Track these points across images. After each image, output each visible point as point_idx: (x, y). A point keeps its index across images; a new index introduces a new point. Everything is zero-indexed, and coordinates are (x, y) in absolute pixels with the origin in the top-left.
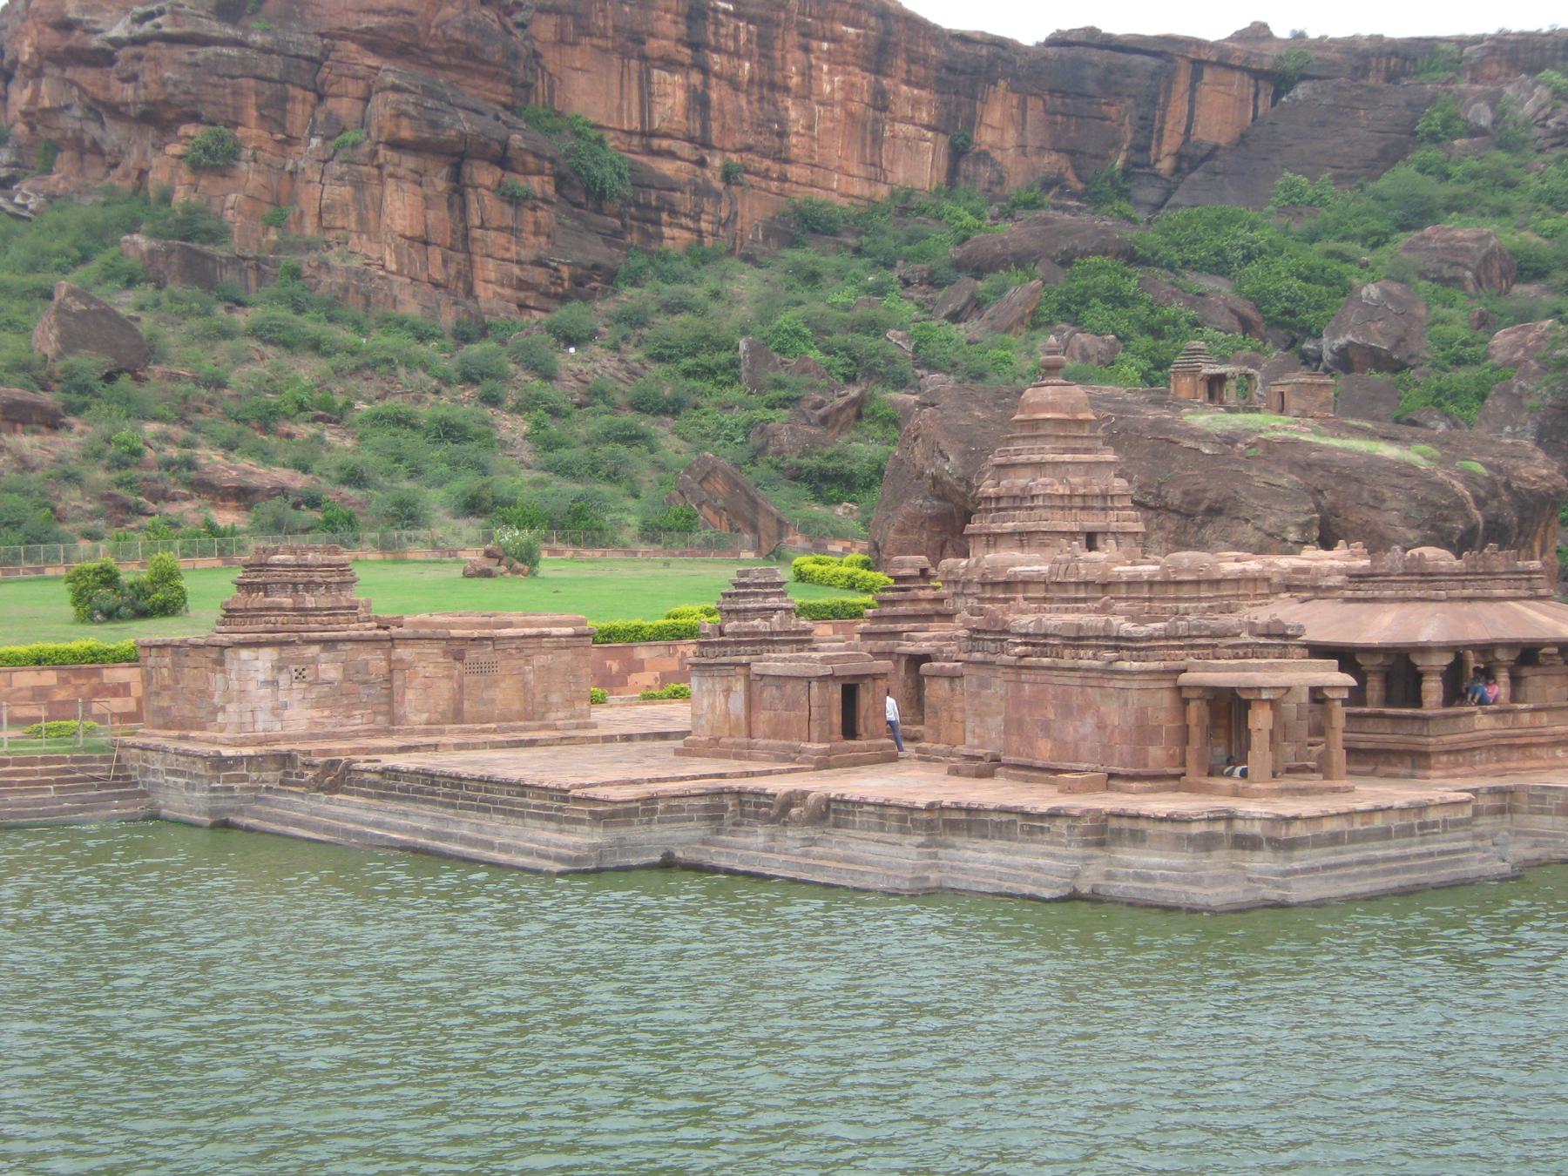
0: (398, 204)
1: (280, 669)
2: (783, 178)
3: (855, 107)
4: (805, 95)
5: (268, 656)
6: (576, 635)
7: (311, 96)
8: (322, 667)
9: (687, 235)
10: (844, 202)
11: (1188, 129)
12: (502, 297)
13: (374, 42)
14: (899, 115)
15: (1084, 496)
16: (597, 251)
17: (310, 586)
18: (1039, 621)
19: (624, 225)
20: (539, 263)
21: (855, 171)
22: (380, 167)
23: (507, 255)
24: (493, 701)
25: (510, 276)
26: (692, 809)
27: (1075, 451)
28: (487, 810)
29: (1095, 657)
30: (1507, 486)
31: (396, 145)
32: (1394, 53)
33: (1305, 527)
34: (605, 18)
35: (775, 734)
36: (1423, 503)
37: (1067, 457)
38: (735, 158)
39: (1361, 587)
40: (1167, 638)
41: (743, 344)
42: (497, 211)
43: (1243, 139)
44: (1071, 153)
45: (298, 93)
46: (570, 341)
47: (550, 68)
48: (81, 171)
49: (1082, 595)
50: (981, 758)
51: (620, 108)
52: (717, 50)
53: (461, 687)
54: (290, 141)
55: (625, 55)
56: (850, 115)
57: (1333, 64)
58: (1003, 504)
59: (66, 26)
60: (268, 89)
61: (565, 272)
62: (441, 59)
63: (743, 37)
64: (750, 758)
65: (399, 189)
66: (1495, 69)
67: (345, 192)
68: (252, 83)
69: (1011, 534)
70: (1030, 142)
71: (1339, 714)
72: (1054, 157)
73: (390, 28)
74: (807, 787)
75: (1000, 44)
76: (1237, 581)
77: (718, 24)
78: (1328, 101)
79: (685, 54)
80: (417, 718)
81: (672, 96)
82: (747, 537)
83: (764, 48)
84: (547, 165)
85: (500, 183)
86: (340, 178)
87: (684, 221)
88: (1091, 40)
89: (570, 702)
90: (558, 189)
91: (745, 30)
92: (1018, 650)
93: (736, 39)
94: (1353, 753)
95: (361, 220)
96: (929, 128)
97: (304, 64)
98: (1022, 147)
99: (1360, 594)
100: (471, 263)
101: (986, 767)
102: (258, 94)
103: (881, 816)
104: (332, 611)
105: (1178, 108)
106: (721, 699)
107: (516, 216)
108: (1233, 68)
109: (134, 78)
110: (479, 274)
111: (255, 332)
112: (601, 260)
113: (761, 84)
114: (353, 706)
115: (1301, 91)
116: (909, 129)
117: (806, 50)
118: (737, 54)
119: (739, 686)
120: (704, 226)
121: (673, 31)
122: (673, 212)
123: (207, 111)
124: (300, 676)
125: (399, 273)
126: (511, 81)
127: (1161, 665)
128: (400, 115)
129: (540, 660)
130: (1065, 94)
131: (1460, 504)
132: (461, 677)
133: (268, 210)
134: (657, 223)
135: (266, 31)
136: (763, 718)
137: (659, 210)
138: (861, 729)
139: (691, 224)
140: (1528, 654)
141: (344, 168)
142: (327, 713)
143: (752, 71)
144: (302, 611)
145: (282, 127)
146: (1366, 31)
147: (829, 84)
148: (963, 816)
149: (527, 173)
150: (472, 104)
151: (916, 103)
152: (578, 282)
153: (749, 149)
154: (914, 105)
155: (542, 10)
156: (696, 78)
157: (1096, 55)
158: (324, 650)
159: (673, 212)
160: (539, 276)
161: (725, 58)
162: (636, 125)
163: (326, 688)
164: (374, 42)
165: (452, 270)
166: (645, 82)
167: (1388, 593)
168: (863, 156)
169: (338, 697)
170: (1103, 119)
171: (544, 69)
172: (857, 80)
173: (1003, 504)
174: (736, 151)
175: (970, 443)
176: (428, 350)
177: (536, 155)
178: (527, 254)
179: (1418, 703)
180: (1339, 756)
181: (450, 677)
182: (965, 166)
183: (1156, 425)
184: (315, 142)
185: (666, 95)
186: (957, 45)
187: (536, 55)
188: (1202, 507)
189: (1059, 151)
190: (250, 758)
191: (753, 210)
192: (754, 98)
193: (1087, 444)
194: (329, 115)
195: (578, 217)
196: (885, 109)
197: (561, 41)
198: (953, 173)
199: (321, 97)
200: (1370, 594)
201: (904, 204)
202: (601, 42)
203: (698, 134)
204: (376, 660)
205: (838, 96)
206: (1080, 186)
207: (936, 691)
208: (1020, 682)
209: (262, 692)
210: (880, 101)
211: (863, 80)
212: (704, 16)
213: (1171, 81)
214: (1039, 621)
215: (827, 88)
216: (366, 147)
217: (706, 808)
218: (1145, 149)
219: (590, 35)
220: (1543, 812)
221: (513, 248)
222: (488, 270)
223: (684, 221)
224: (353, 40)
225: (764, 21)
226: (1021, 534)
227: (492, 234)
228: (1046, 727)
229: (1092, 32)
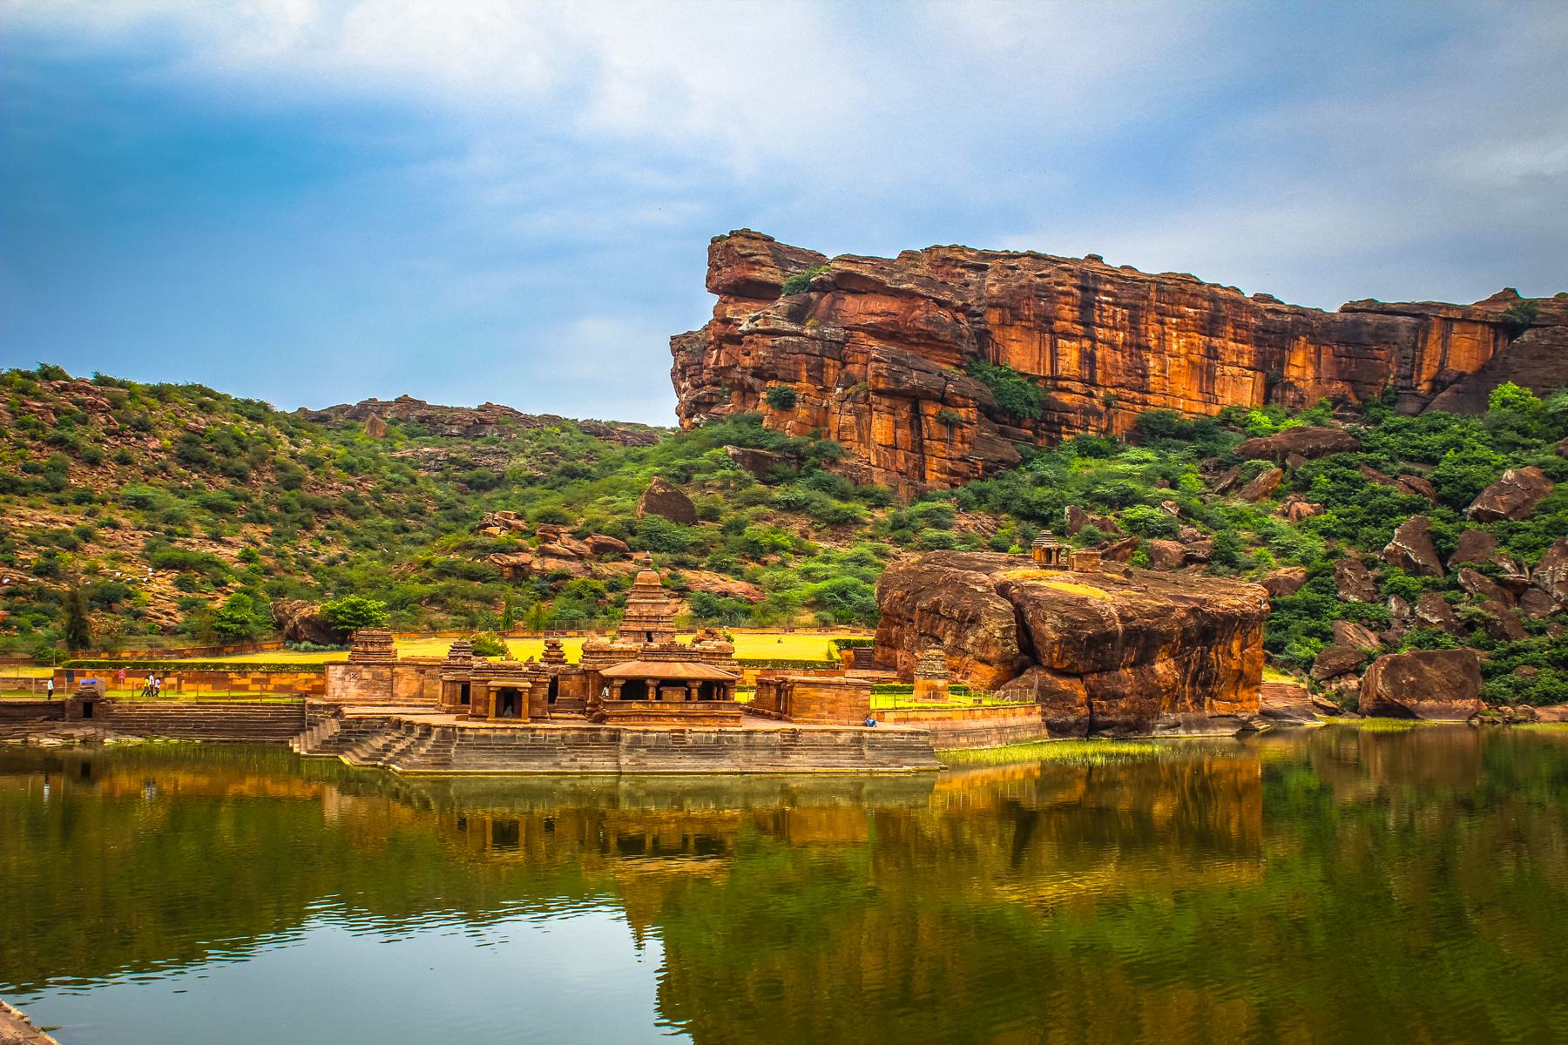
2: (1145, 403)
3: (1194, 358)
4: (1159, 352)
5: (341, 669)
11: (1442, 363)
13: (875, 332)
16: (1007, 450)
17: (372, 644)
19: (1036, 434)
20: (963, 459)
31: (878, 392)
38: (1112, 391)
44: (1351, 381)
45: (831, 362)
48: (743, 402)
54: (826, 390)
55: (1042, 331)
56: (1191, 362)
57: (1553, 316)
59: (727, 322)
63: (1119, 317)
65: (879, 417)
67: (851, 419)
75: (1299, 312)
81: (1070, 354)
88: (1371, 307)
93: (1114, 319)
95: (860, 436)
98: (1317, 379)
104: (380, 653)
105: (1433, 349)
108: (1475, 322)
109: (748, 354)
110: (928, 466)
115: (1527, 336)
116: (1235, 370)
117: (1162, 323)
118: (1115, 328)
121: (1070, 316)
122: (1069, 426)
123: (780, 374)
128: (878, 375)
130: (1348, 344)
133: (811, 430)
134: (1060, 432)
135: (812, 327)
137: (1060, 424)
144: (367, 653)
147: (1177, 344)
151: (1240, 354)
153: (1122, 386)
155: (992, 306)
156: (1086, 344)
157: (1370, 318)
159: (1069, 426)
160: (962, 467)
161: (1107, 331)
162: (1048, 373)
164: (875, 332)
166: (1054, 347)
172: (1196, 341)
178: (955, 454)
184: (839, 390)
189: (1343, 381)
194: (847, 374)
197: (1003, 324)
198: (1267, 398)
199: (845, 364)
204: (386, 672)
205: (1183, 351)
206: (1355, 402)
210: (1212, 354)
211: (1199, 340)
212: (1093, 306)
213: (1426, 333)
215: (1175, 347)
222: (934, 464)
225: (1134, 307)
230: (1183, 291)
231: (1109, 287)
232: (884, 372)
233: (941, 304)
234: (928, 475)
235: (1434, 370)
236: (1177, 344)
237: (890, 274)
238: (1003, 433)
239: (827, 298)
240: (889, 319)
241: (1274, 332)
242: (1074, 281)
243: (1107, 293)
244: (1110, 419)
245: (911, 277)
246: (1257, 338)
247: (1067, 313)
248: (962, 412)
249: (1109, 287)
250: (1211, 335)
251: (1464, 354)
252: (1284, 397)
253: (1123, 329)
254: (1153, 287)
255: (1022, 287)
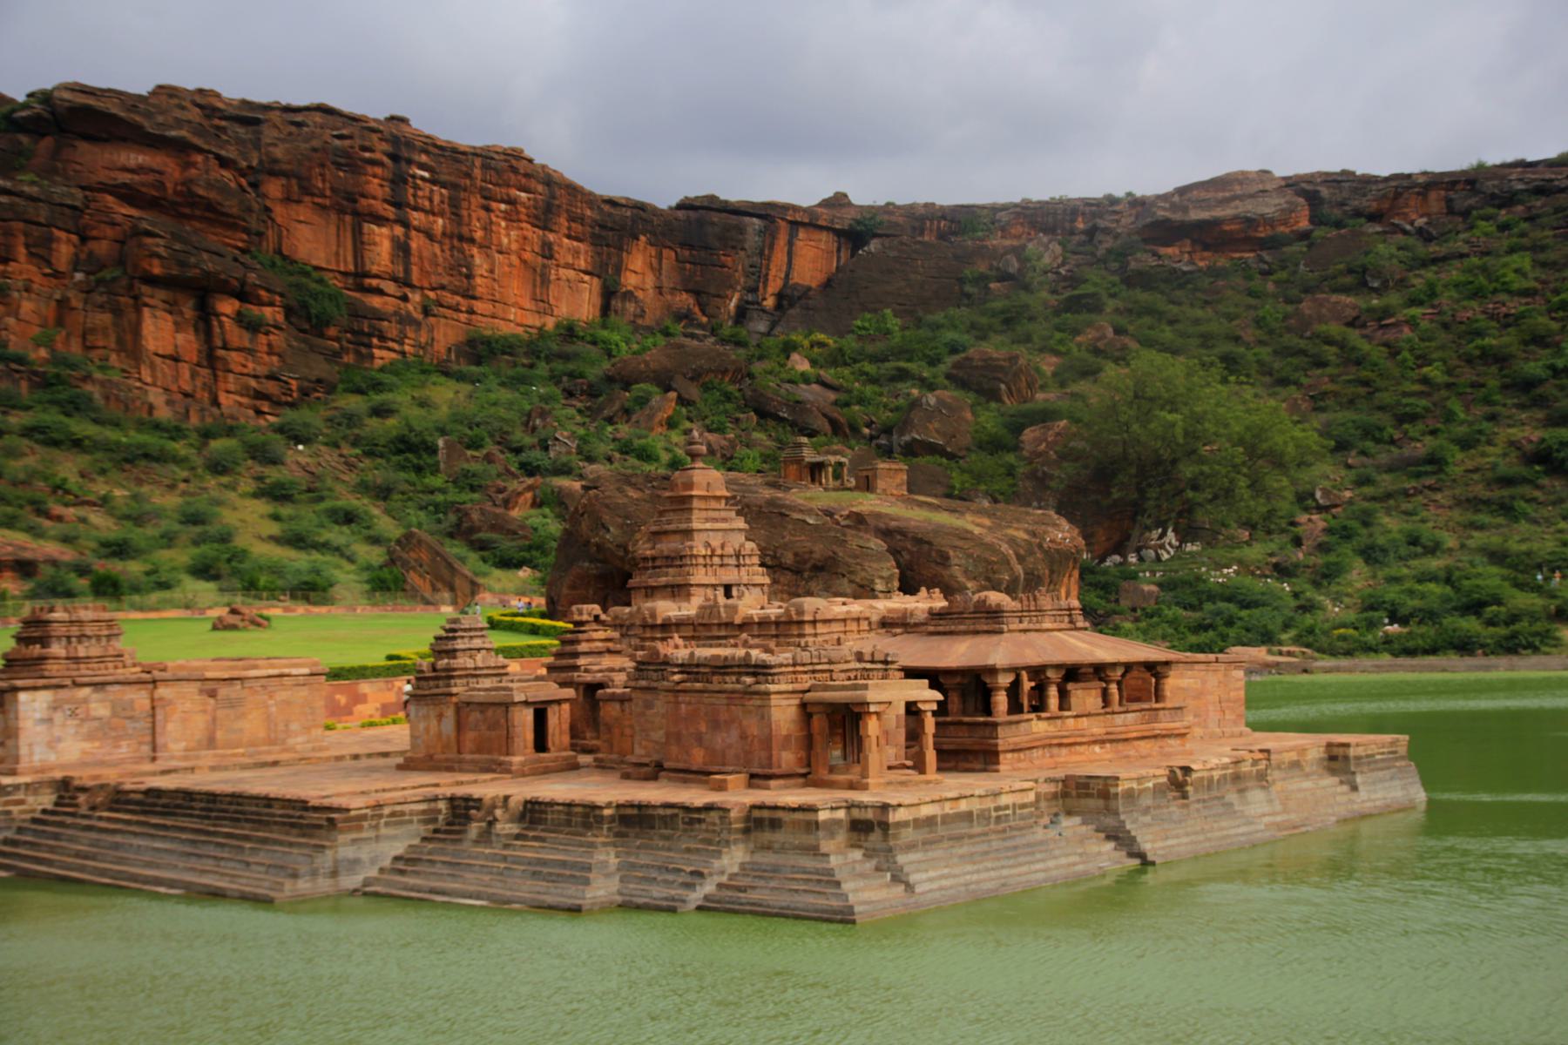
0: (152, 328)
1: (55, 709)
2: (471, 312)
3: (527, 256)
4: (484, 247)
5: (44, 697)
6: (312, 675)
7: (74, 238)
8: (93, 705)
9: (394, 355)
10: (520, 330)
11: (787, 275)
12: (240, 404)
14: (562, 262)
15: (722, 556)
18: (692, 654)
20: (272, 377)
21: (528, 306)
22: (136, 298)
23: (245, 371)
24: (241, 730)
25: (247, 388)
26: (412, 813)
27: (715, 520)
28: (238, 820)
29: (738, 682)
30: (1040, 546)
32: (944, 217)
33: (888, 580)
34: (324, 181)
35: (479, 750)
36: (978, 560)
37: (708, 526)
38: (432, 294)
39: (940, 624)
40: (794, 665)
41: (441, 443)
42: (236, 335)
43: (828, 284)
44: (697, 293)
45: (63, 235)
46: (298, 440)
47: (279, 220)
49: (723, 633)
50: (646, 765)
51: (337, 254)
52: (415, 209)
53: (214, 719)
55: (341, 211)
56: (524, 262)
57: (897, 224)
58: (658, 563)
60: (36, 231)
61: (294, 384)
62: (187, 211)
64: (461, 770)
66: (1020, 229)
67: (106, 318)
68: (21, 225)
69: (665, 587)
70: (665, 284)
71: (930, 724)
72: (685, 296)
73: (143, 185)
74: (508, 792)
75: (641, 207)
76: (844, 620)
77: (416, 187)
78: (892, 254)
79: (390, 212)
80: (177, 747)
82: (447, 595)
83: (455, 209)
84: (278, 298)
85: (239, 313)
86: (101, 307)
87: (391, 344)
89: (307, 729)
90: (287, 317)
91: (440, 193)
92: (677, 677)
93: (431, 200)
94: (941, 753)
95: (120, 342)
96: (586, 272)
97: (67, 211)
98: (659, 289)
99: (941, 629)
100: (215, 376)
101: (654, 771)
102: (26, 234)
103: (569, 814)
104: (101, 659)
105: (780, 257)
106: (434, 722)
107: (251, 341)
108: (821, 228)
110: (222, 385)
111: (28, 432)
112: (324, 375)
113: (451, 237)
114: (118, 738)
115: (874, 246)
116: (571, 274)
117: (488, 209)
119: (450, 713)
120: (407, 348)
122: (382, 338)
124: (73, 714)
125: (154, 385)
126: (247, 231)
127: (790, 687)
129: (282, 695)
130: (691, 247)
131: (1006, 561)
132: (215, 710)
134: (370, 346)
136: (470, 736)
137: (370, 335)
138: (550, 745)
139: (396, 346)
140: (1072, 673)
141: (105, 298)
142: (97, 744)
143: (444, 226)
144: (77, 660)
145: (49, 264)
146: (922, 199)
148: (635, 812)
149: (261, 304)
150: (214, 249)
152: (305, 393)
153: (443, 287)
154: (574, 254)
155: (273, 173)
156: (399, 231)
158: (95, 691)
159: (382, 338)
160: (272, 387)
162: (351, 268)
163: (96, 724)
164: (128, 195)
165: (199, 383)
166: (357, 233)
167: (962, 628)
168: (534, 293)
169: (104, 731)
170: (723, 266)
171: (273, 220)
172: (530, 235)
173: (658, 563)
174: (433, 289)
175: (627, 517)
176: (179, 447)
177: (268, 290)
178: (262, 370)
179: (988, 710)
180: (931, 756)
181: (204, 711)
182: (616, 303)
183: (772, 503)
185: (375, 244)
186: (606, 208)
187: (268, 209)
188: (809, 565)
189: (687, 291)
190: (27, 785)
191: (446, 334)
192: (446, 247)
193: (723, 514)
194: (91, 254)
195: (305, 341)
196: (551, 257)
198: (605, 310)
200: (947, 629)
201: (569, 332)
202: (320, 200)
203: (401, 275)
204: (140, 698)
205: (514, 246)
206: (705, 319)
207: (610, 711)
208: (678, 703)
209: (39, 728)
210: (547, 251)
211: (534, 234)
212: (405, 182)
213: (774, 237)
214: (692, 654)
215: (505, 241)
216: (124, 282)
217: (424, 812)
218: (754, 290)
219: (313, 195)
220: (1088, 796)
221: (251, 365)
223: (391, 344)
224: (111, 194)
225: (453, 186)
226: (673, 586)
227: (234, 354)
228: (699, 739)
229: (712, 198)
230: (514, 170)
231: (424, 158)
232: (161, 251)
233: (224, 163)
234: (223, 398)
235: (780, 283)
236: (507, 237)
237: (148, 115)
238: (312, 348)
239: (47, 143)
240: (151, 178)
241: (616, 226)
242: (385, 147)
243: (422, 166)
244: (431, 330)
245: (179, 123)
246: (593, 235)
247: (376, 186)
248: (268, 311)
249: (424, 158)
250: (545, 228)
251: (811, 262)
252: (624, 309)
253: (442, 214)
254: (478, 162)
255: (315, 150)
